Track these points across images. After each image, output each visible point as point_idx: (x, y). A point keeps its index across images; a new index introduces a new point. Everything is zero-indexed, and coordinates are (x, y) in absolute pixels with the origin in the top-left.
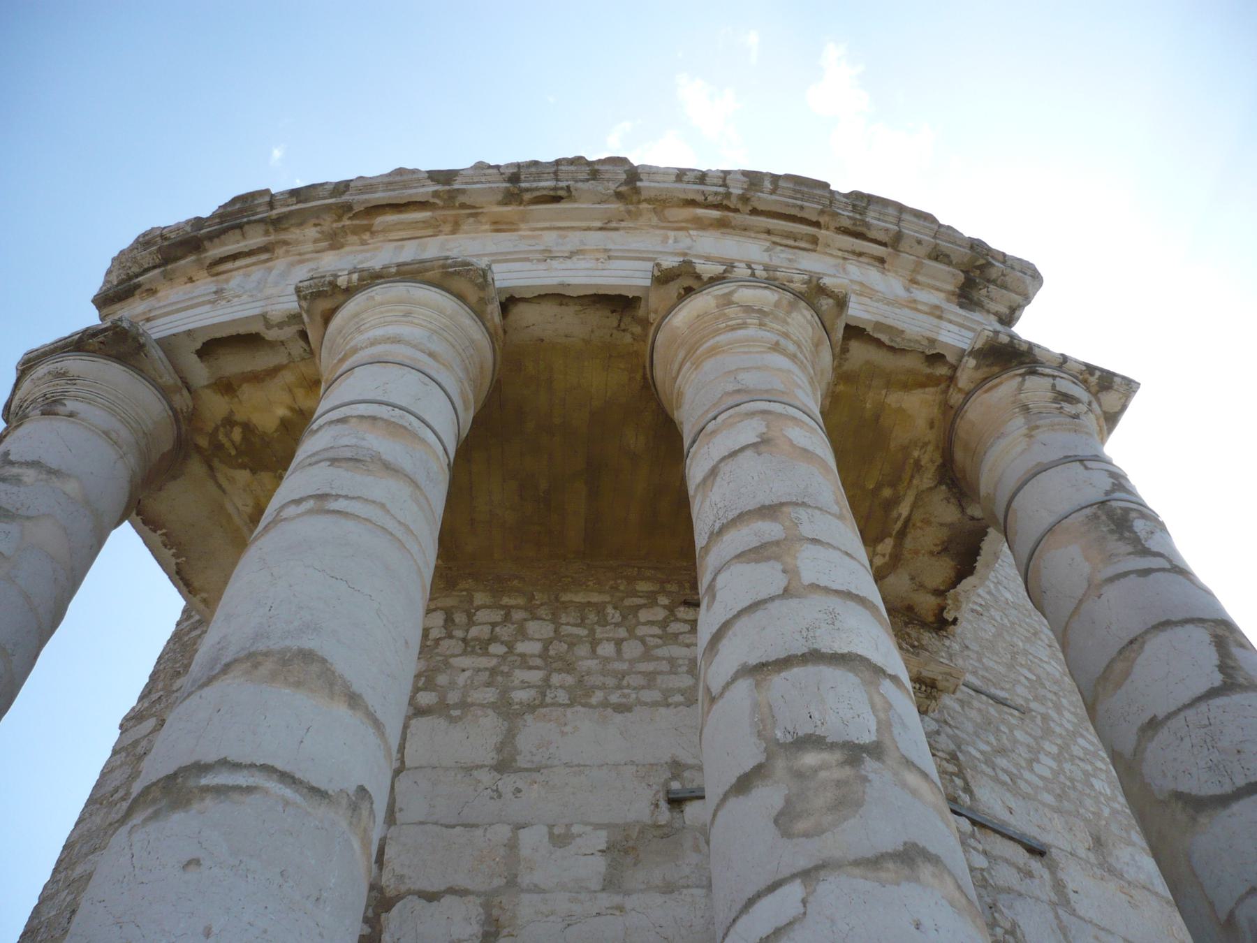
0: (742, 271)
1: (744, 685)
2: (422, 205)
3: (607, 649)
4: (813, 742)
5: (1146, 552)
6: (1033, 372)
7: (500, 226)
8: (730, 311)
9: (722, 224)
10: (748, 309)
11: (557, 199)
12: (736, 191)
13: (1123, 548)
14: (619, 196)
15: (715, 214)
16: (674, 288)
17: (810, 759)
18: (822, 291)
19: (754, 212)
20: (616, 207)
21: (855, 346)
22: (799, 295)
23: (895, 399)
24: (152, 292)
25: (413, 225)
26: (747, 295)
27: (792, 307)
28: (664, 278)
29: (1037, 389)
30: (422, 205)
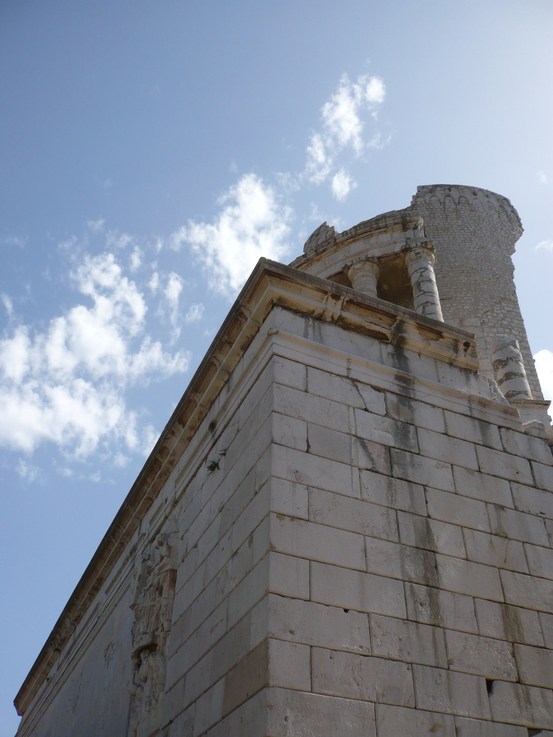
0: (355, 261)
2: (304, 263)
5: (421, 291)
6: (411, 251)
7: (318, 260)
8: (355, 270)
9: (354, 241)
10: (358, 269)
11: (325, 251)
12: (353, 234)
14: (334, 245)
15: (352, 239)
16: (346, 269)
18: (369, 258)
19: (359, 235)
20: (335, 247)
21: (382, 259)
22: (365, 261)
23: (394, 262)
25: (305, 267)
26: (357, 266)
27: (364, 264)
28: (344, 268)
29: (412, 254)
30: (304, 263)
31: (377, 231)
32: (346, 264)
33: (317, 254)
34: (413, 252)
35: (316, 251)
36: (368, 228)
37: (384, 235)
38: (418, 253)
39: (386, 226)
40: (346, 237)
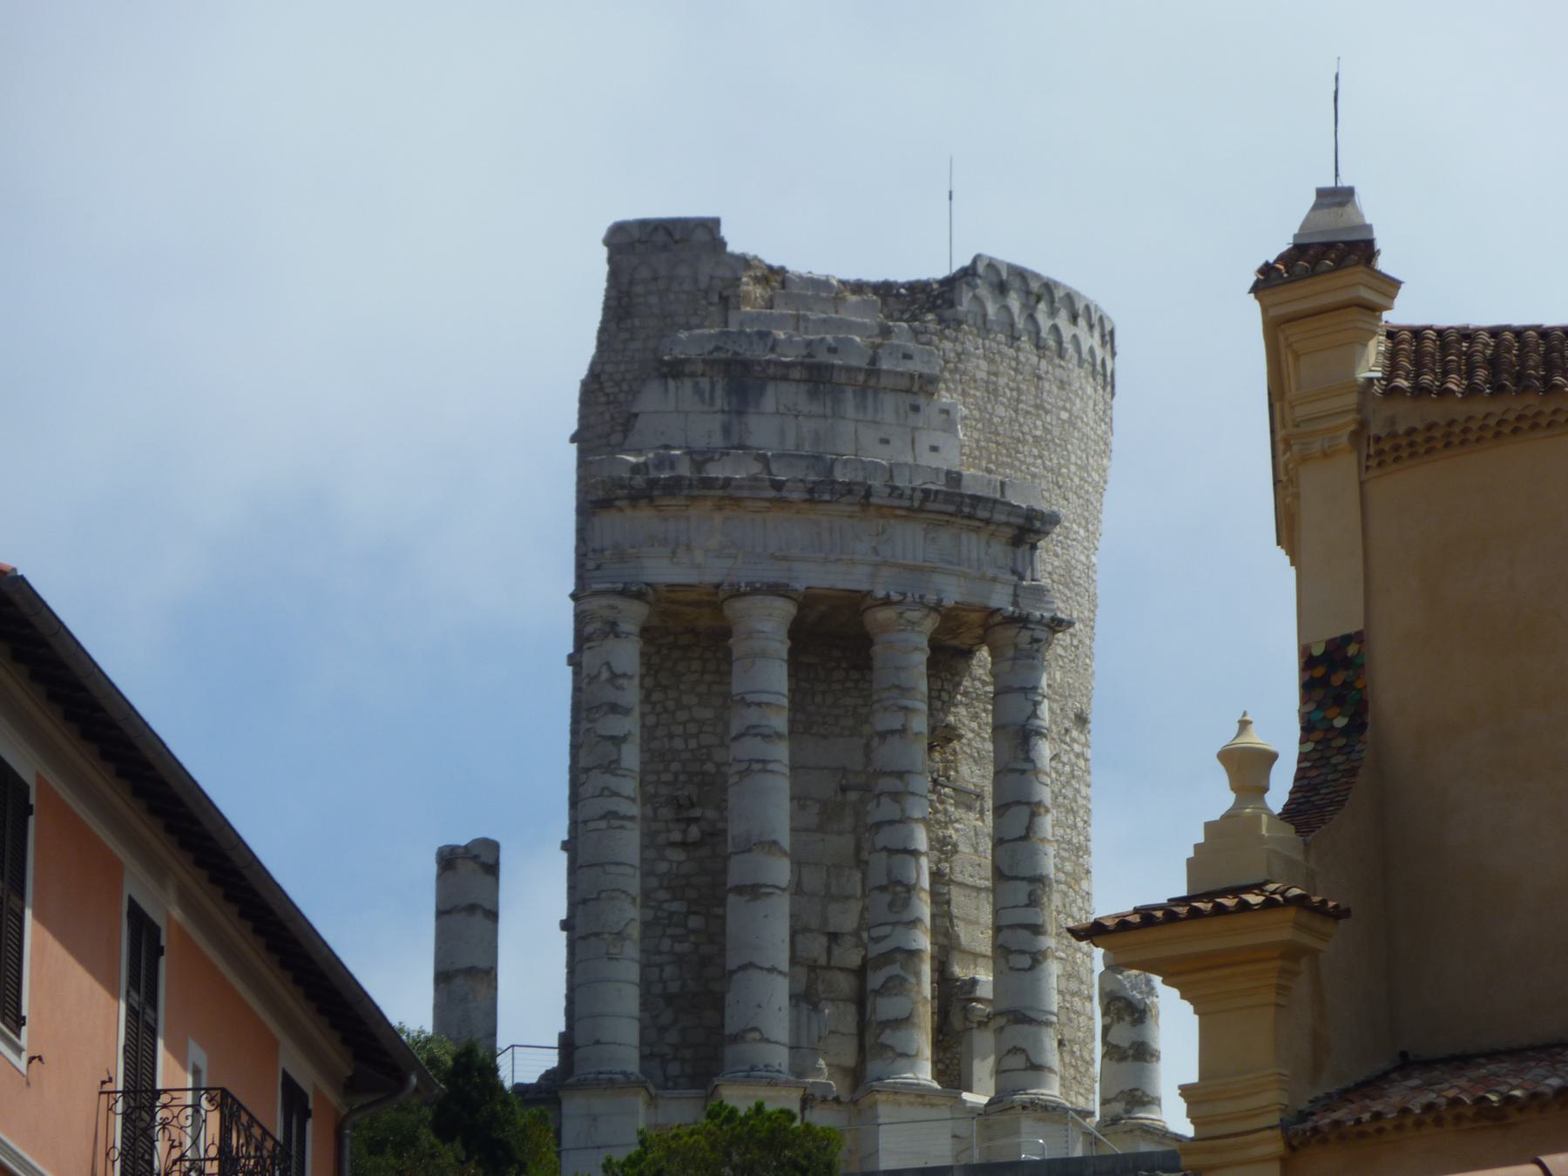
0: (910, 598)
1: (884, 854)
3: (818, 699)
4: (899, 883)
6: (1025, 627)
13: (1022, 756)
17: (899, 889)
24: (621, 510)
29: (1025, 636)
31: (966, 522)
32: (888, 596)
33: (811, 501)
34: (1029, 633)
35: (811, 491)
36: (951, 508)
37: (974, 536)
38: (1037, 641)
39: (988, 522)
40: (896, 503)
